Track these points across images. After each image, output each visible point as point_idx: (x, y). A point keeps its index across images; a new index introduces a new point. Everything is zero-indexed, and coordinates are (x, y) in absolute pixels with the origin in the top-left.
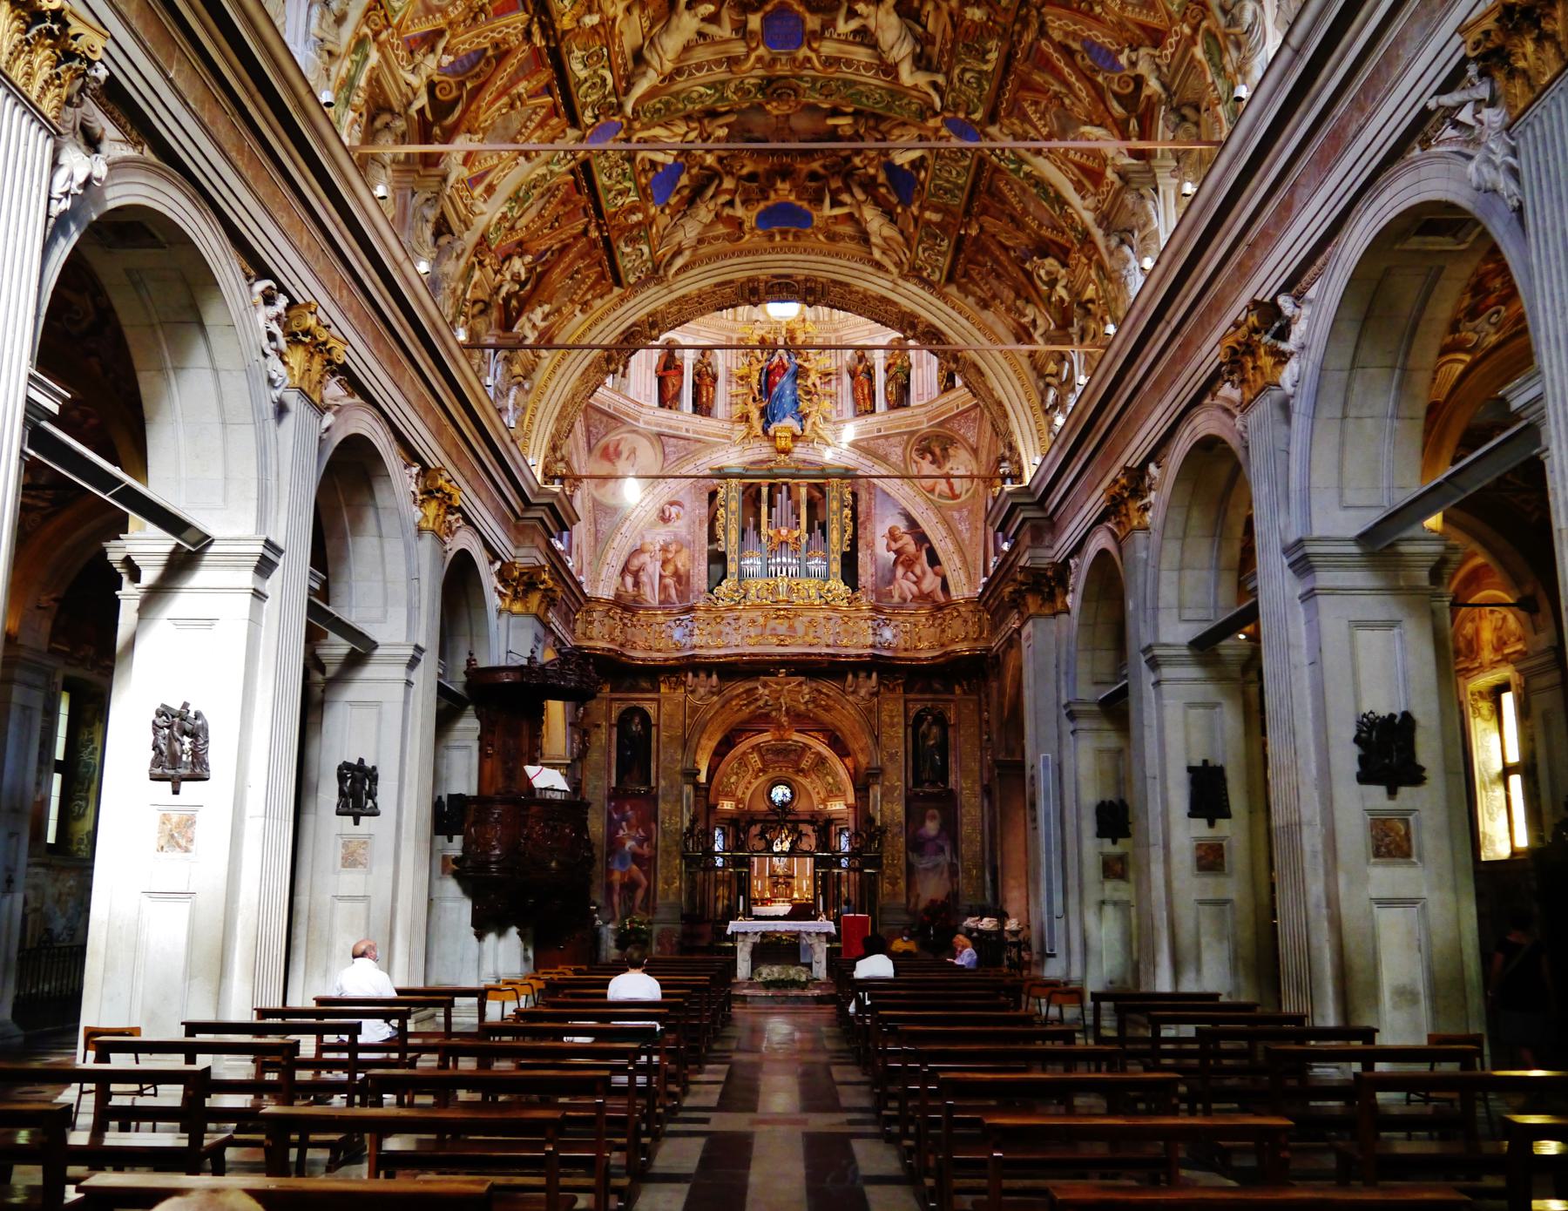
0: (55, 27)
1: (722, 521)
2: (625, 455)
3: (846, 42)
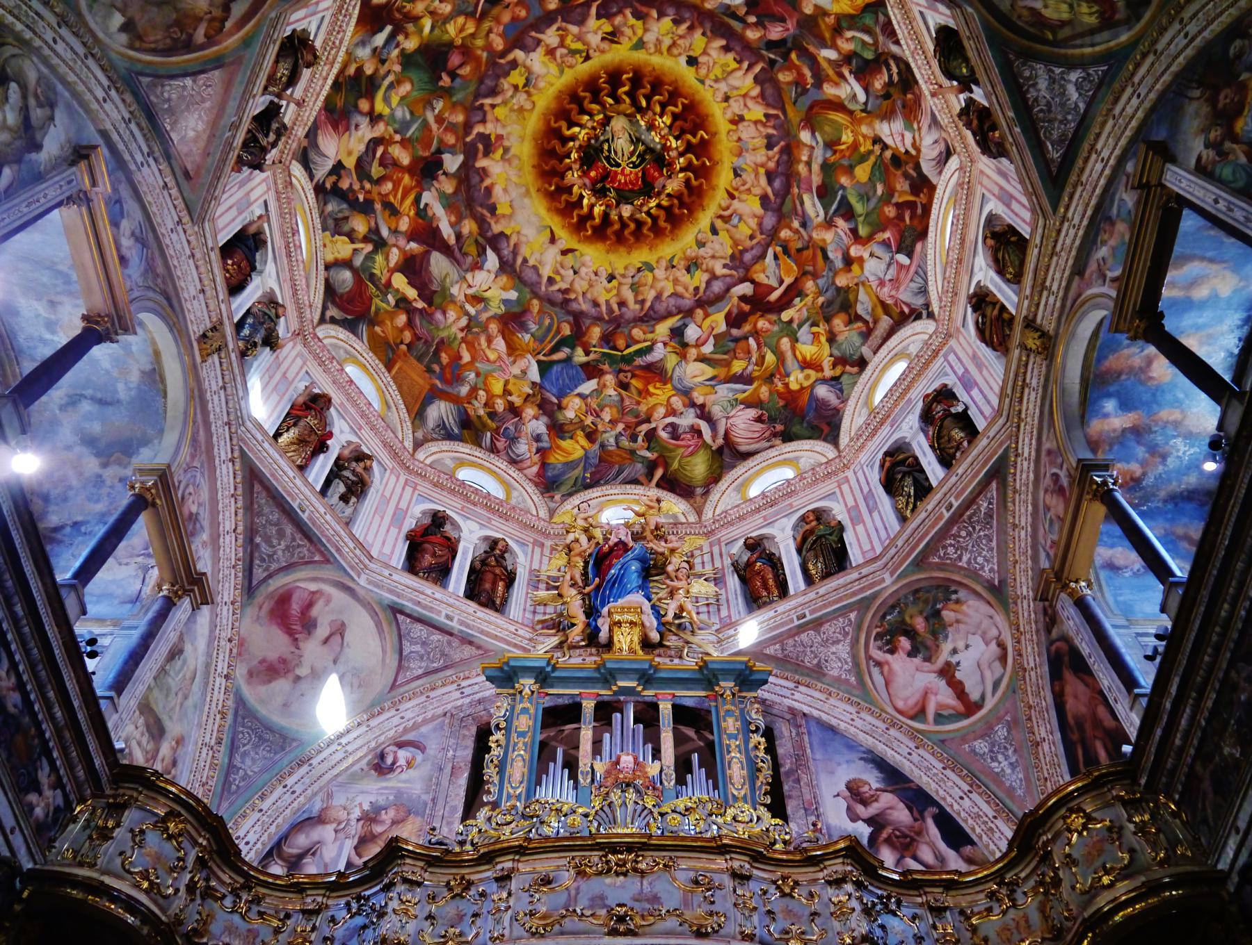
1: (496, 752)
2: (322, 631)
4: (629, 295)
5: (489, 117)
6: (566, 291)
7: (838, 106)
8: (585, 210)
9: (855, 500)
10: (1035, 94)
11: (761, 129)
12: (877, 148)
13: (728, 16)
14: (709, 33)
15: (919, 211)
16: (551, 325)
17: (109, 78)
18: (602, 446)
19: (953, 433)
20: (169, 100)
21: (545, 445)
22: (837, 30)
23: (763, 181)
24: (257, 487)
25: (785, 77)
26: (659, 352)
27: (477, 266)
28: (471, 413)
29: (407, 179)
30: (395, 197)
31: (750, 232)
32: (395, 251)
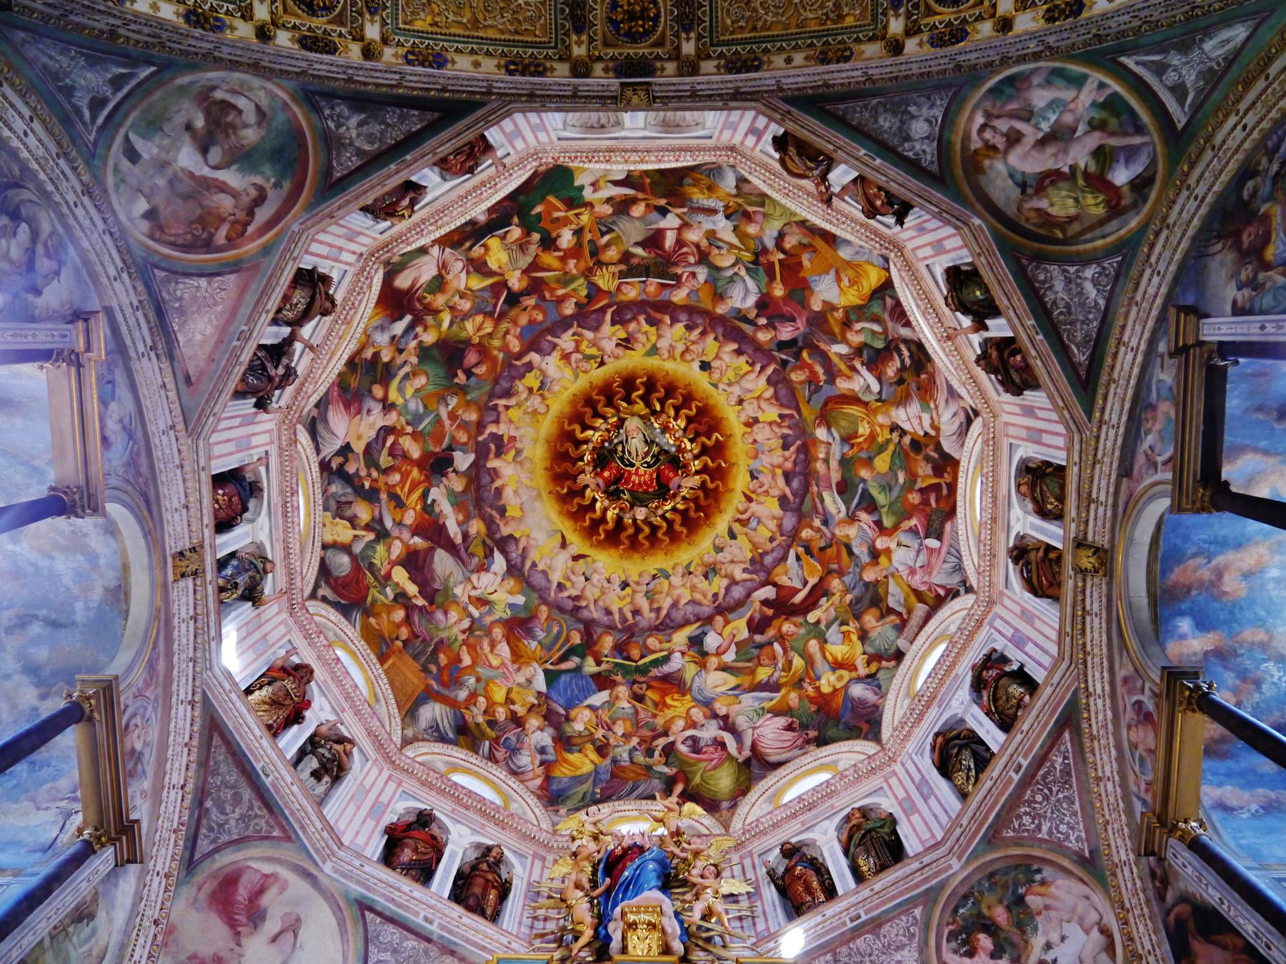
2: (272, 925)
4: (643, 604)
5: (503, 418)
6: (577, 598)
7: (853, 399)
8: (598, 512)
9: (906, 791)
10: (1053, 297)
11: (777, 430)
12: (895, 436)
13: (739, 319)
14: (721, 338)
15: (945, 492)
16: (559, 633)
17: (124, 261)
18: (615, 761)
19: (1011, 690)
20: (181, 299)
21: (550, 757)
22: (847, 324)
23: (781, 481)
24: (216, 740)
25: (797, 377)
26: (677, 662)
27: (483, 568)
28: (469, 720)
29: (415, 473)
30: (402, 489)
31: (769, 535)
32: (397, 543)
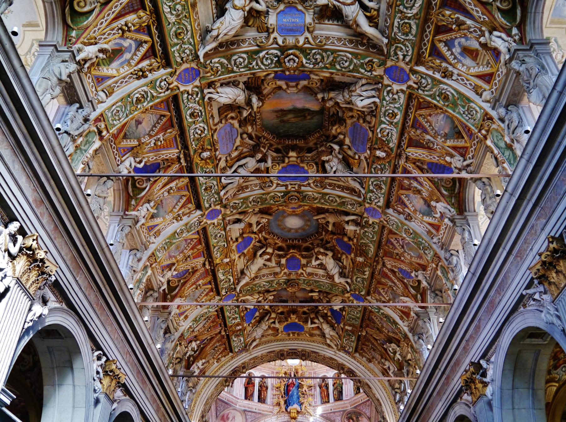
0: (40, 264)
2: (230, 419)
3: (315, 268)
